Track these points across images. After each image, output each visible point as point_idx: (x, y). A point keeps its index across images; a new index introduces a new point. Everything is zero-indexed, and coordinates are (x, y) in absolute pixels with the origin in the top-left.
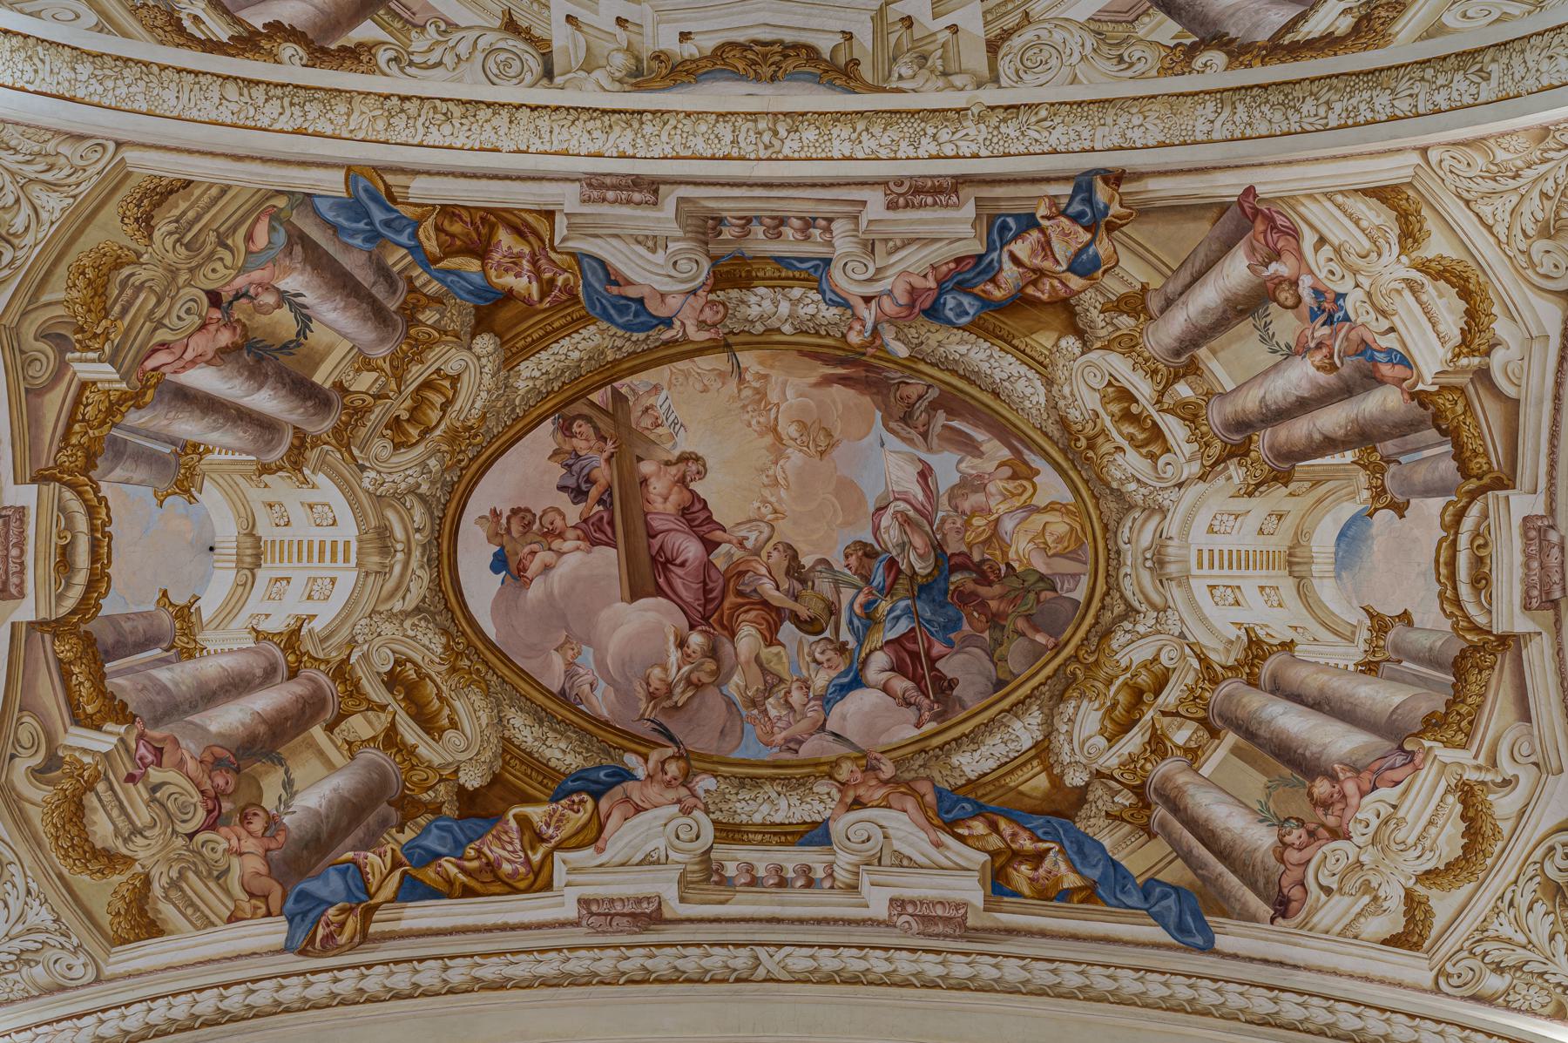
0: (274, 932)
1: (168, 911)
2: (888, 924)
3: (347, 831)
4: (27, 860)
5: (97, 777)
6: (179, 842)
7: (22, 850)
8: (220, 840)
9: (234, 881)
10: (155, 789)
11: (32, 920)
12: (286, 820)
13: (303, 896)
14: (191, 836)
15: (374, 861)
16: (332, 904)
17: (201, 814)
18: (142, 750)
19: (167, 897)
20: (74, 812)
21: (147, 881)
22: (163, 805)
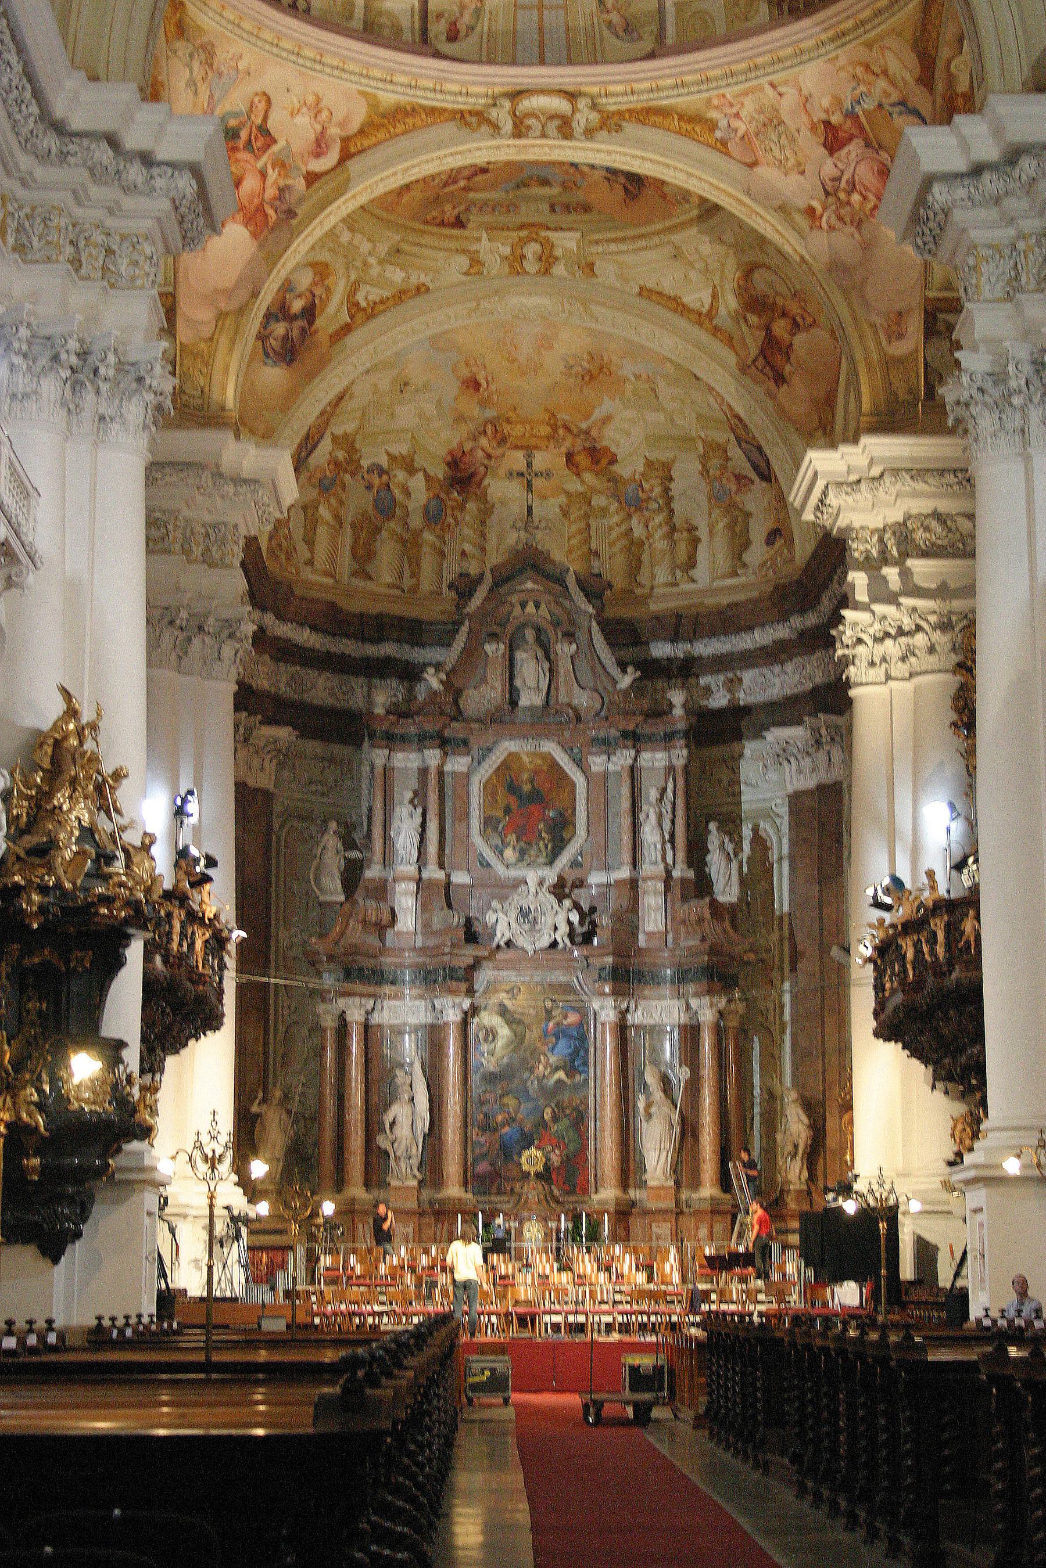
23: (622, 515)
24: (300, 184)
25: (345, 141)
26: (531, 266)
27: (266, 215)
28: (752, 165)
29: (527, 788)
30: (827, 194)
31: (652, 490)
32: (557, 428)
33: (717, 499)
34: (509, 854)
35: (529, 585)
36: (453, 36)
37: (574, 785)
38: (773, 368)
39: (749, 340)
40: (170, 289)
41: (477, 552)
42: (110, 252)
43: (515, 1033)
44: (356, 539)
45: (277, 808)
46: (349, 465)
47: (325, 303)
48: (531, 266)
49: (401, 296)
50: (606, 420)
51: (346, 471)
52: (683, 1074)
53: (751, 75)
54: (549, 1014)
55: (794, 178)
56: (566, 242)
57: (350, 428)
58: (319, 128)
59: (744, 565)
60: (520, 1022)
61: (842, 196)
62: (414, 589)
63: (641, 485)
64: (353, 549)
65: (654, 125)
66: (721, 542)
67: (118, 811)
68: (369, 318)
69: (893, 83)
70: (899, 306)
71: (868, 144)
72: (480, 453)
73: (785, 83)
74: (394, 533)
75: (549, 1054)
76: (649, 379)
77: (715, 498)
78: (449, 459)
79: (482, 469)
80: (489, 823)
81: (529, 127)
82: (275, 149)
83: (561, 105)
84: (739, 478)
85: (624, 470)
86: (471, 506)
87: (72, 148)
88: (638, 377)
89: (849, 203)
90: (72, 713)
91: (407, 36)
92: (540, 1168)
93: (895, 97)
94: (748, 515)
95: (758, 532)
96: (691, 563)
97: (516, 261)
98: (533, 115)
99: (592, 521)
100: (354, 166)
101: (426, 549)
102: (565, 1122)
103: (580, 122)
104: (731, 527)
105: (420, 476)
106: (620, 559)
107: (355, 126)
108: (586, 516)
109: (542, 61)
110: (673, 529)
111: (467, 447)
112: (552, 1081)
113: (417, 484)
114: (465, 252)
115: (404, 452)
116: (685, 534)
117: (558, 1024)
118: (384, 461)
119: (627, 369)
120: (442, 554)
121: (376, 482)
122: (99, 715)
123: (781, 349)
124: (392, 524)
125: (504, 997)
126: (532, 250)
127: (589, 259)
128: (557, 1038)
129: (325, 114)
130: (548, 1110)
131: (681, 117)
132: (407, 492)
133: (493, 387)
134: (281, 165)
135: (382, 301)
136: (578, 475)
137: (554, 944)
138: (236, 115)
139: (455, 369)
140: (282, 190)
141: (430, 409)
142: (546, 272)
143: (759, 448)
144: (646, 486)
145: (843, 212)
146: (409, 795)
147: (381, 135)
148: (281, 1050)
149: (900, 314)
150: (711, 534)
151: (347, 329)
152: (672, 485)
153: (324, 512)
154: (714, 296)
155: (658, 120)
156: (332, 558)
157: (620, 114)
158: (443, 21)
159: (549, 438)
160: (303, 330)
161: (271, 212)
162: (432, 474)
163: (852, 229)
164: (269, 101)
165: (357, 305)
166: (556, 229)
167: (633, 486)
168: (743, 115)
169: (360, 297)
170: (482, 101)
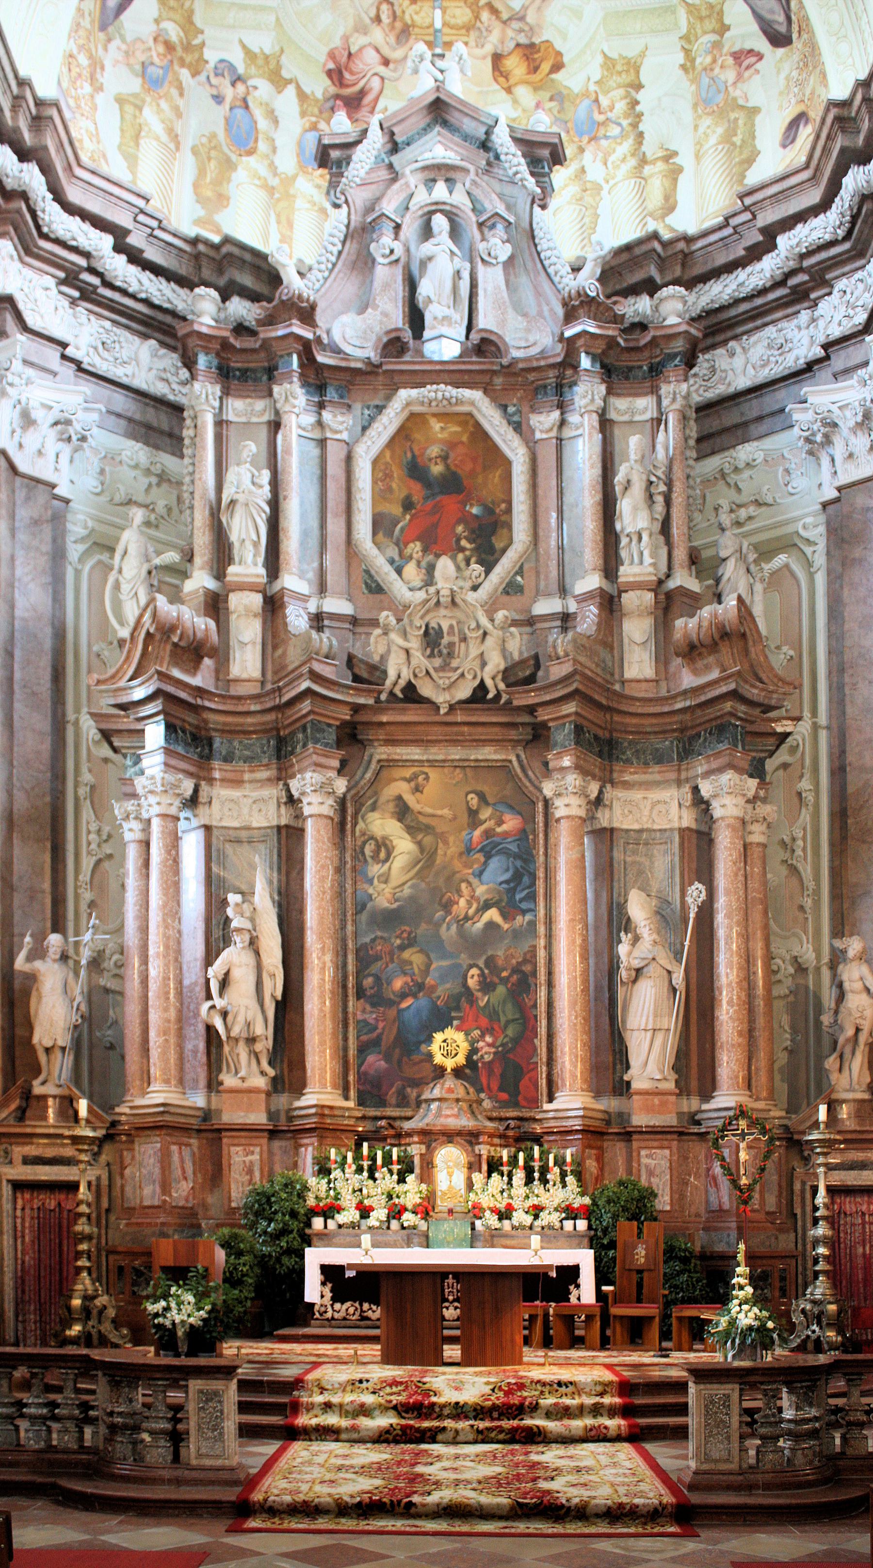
31: (612, 108)
33: (706, 102)
34: (410, 569)
43: (419, 844)
44: (202, 172)
51: (182, 63)
60: (428, 829)
63: (597, 101)
72: (371, 56)
74: (256, 175)
75: (475, 881)
77: (701, 103)
78: (331, 66)
79: (375, 83)
101: (300, 203)
102: (501, 990)
105: (290, 91)
111: (357, 42)
112: (480, 925)
115: (267, 51)
117: (488, 834)
118: (238, 59)
121: (229, 93)
124: (252, 161)
125: (401, 788)
128: (488, 856)
130: (474, 971)
136: (509, 90)
144: (604, 102)
152: (640, 96)
162: (307, 90)
167: (586, 103)
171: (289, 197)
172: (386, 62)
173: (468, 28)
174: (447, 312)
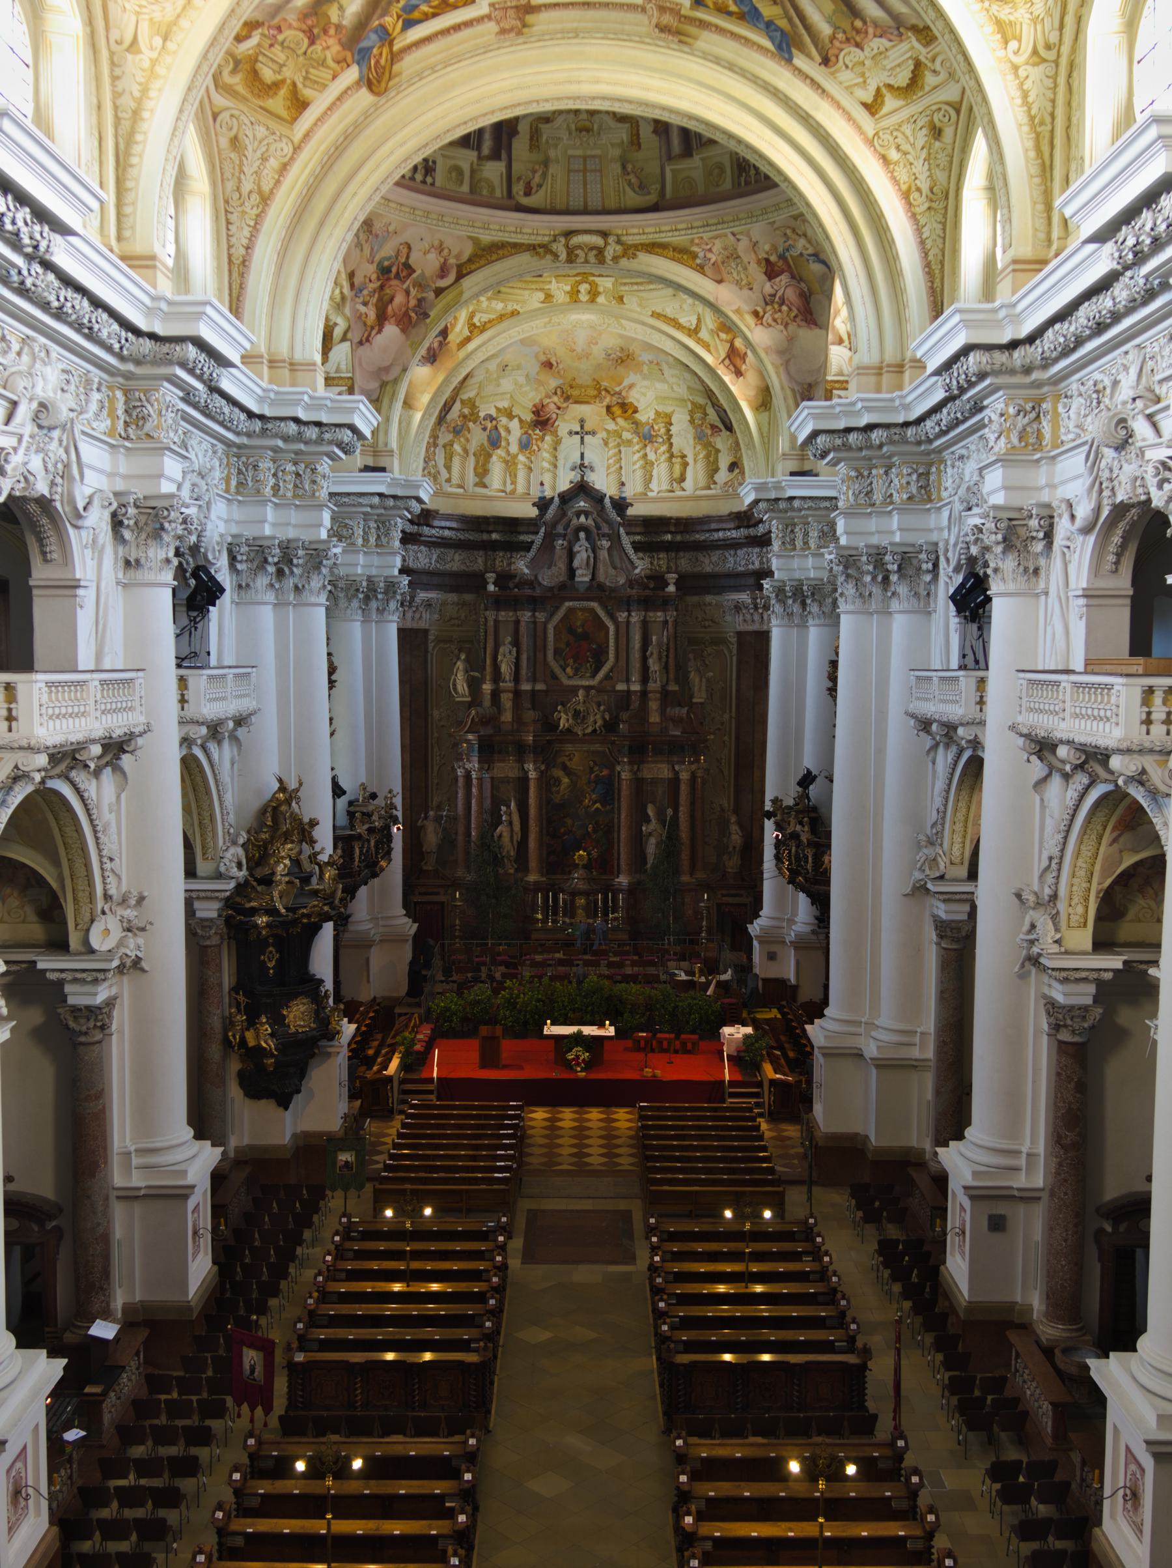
0: (352, 74)
1: (307, 93)
2: (644, 10)
3: (373, 13)
4: (245, 109)
5: (257, 55)
6: (301, 58)
7: (242, 107)
8: (318, 47)
9: (330, 62)
10: (282, 43)
11: (259, 136)
12: (344, 23)
13: (360, 51)
14: (305, 53)
15: (388, 20)
16: (373, 47)
17: (306, 41)
18: (272, 32)
19: (305, 86)
20: (255, 74)
21: (294, 84)
22: (289, 48)
23: (641, 445)
24: (431, 295)
25: (460, 267)
26: (584, 297)
27: (410, 317)
28: (720, 282)
29: (580, 630)
30: (767, 304)
32: (599, 391)
33: (700, 439)
34: (569, 670)
35: (582, 504)
36: (528, 193)
37: (608, 628)
38: (735, 366)
39: (720, 347)
40: (350, 375)
41: (551, 468)
42: (298, 475)
44: (477, 462)
45: (431, 637)
46: (473, 416)
47: (454, 326)
48: (584, 297)
49: (502, 317)
50: (631, 387)
52: (670, 812)
53: (720, 227)
54: (591, 770)
55: (746, 292)
56: (605, 283)
57: (472, 394)
58: (442, 260)
59: (715, 483)
61: (776, 306)
62: (513, 492)
64: (475, 469)
65: (657, 254)
66: (701, 465)
67: (315, 842)
68: (482, 332)
69: (810, 242)
70: (809, 380)
71: (793, 277)
72: (552, 406)
73: (741, 233)
76: (658, 364)
79: (554, 416)
80: (557, 652)
81: (577, 256)
82: (414, 275)
83: (598, 241)
84: (713, 427)
85: (643, 417)
86: (548, 438)
87: (270, 426)
88: (651, 362)
89: (780, 311)
90: (282, 788)
91: (498, 194)
92: (585, 862)
93: (811, 251)
94: (718, 451)
95: (724, 462)
96: (682, 479)
97: (574, 294)
98: (579, 247)
99: (622, 449)
100: (467, 282)
101: (520, 466)
103: (609, 253)
104: (707, 456)
105: (516, 420)
106: (639, 473)
107: (465, 257)
108: (619, 445)
109: (585, 211)
110: (672, 456)
111: (546, 401)
113: (514, 425)
114: (541, 290)
116: (679, 460)
118: (493, 412)
119: (645, 357)
120: (530, 469)
122: (301, 784)
123: (739, 355)
124: (499, 451)
126: (584, 288)
127: (621, 293)
129: (446, 252)
131: (674, 250)
132: (508, 431)
133: (561, 366)
134: (419, 285)
135: (490, 321)
136: (614, 419)
137: (595, 731)
138: (388, 259)
139: (536, 356)
140: (420, 301)
141: (522, 380)
142: (592, 301)
143: (725, 411)
144: (656, 427)
145: (776, 316)
146: (509, 639)
147: (482, 262)
148: (436, 781)
149: (810, 385)
150: (695, 461)
151: (468, 340)
153: (457, 448)
154: (699, 320)
155: (660, 251)
156: (462, 477)
157: (636, 247)
158: (521, 182)
159: (595, 397)
160: (441, 343)
161: (413, 315)
163: (782, 327)
164: (409, 248)
165: (474, 325)
166: (599, 276)
167: (647, 428)
168: (715, 249)
169: (476, 320)
170: (547, 239)
171: (515, 464)
172: (559, 408)
173: (595, 397)
174: (585, 572)
